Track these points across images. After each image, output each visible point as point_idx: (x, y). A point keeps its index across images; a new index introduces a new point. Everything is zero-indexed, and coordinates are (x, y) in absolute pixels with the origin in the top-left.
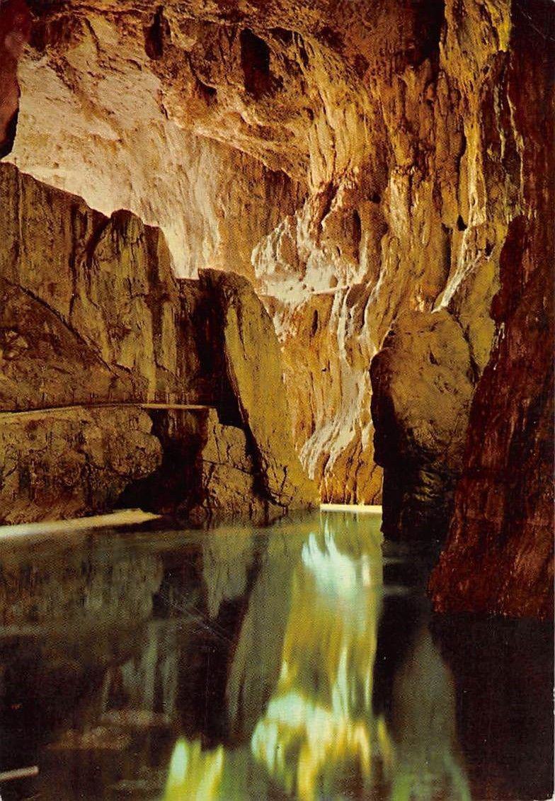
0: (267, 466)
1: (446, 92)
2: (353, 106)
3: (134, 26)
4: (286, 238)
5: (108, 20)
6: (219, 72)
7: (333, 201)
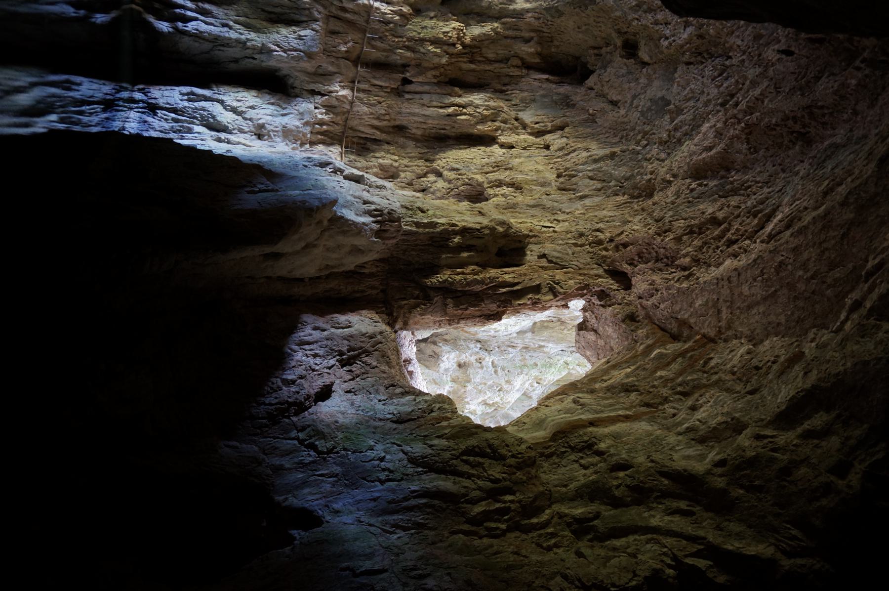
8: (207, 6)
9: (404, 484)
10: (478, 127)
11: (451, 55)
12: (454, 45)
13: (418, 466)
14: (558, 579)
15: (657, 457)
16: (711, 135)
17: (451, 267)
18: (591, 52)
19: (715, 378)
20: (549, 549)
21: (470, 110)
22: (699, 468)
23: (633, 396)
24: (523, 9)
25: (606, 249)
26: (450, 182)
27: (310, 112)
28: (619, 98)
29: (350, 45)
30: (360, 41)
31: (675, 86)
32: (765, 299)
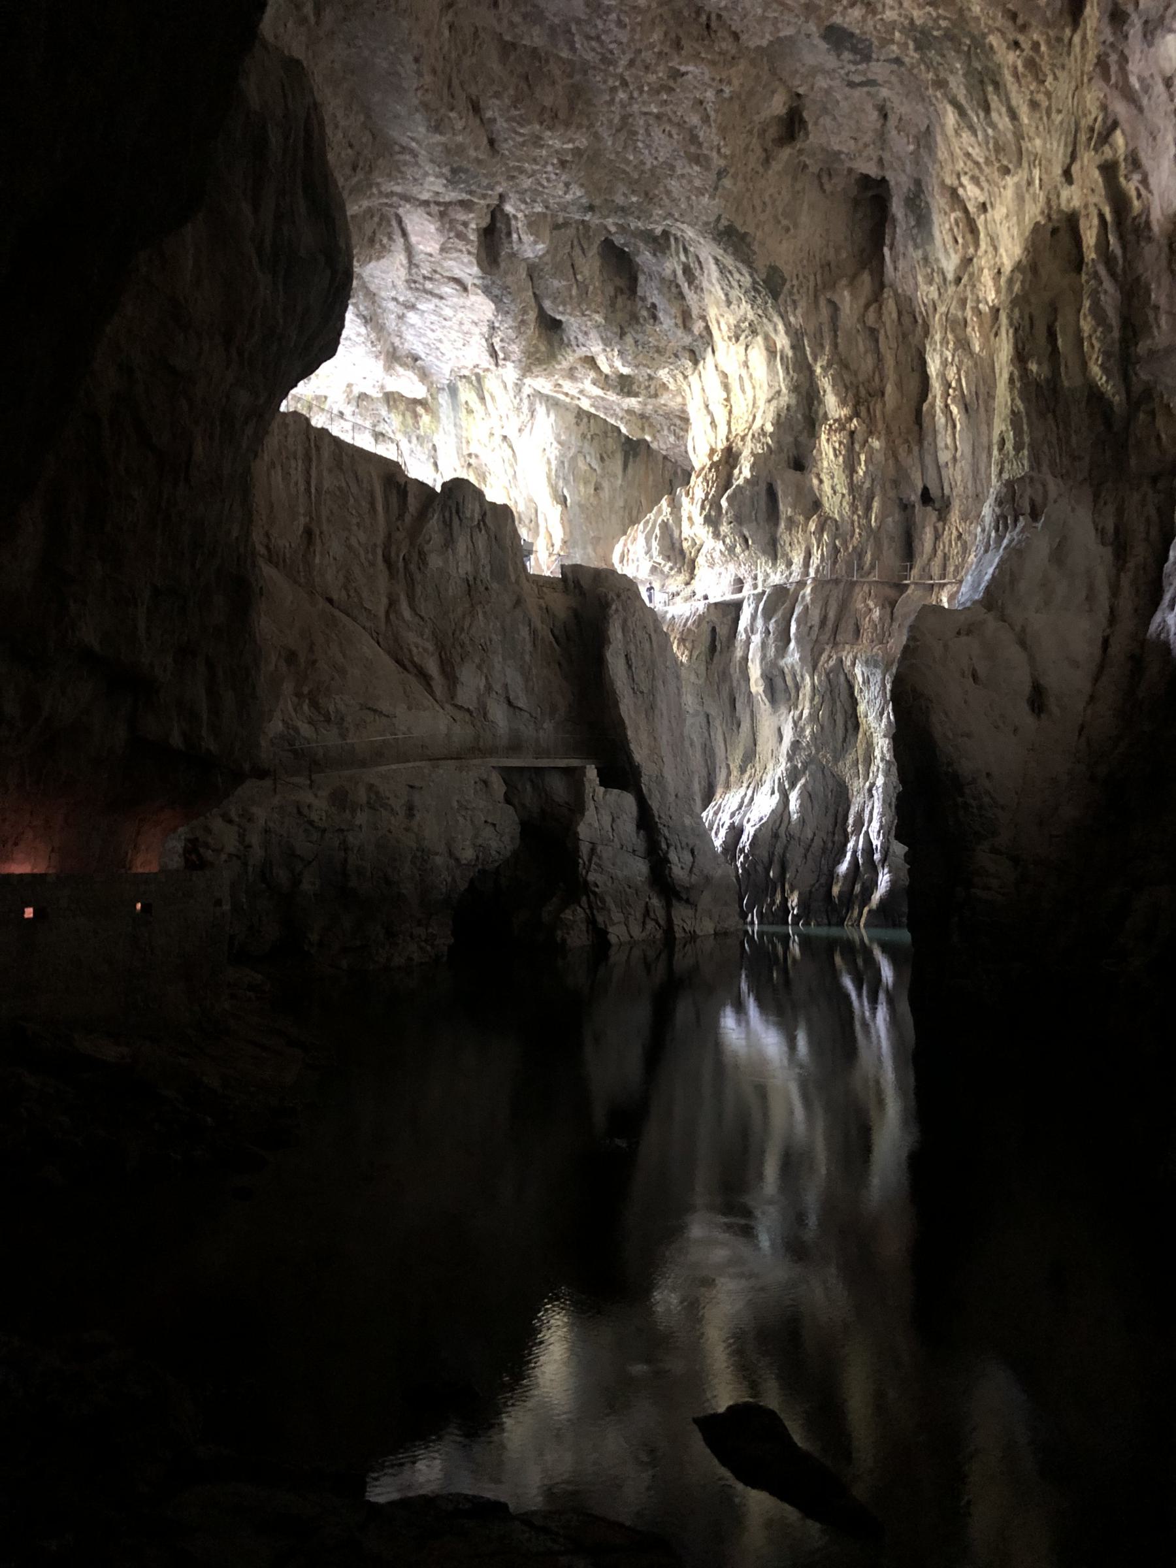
0: (668, 846)
1: (895, 315)
2: (760, 339)
3: (465, 224)
4: (665, 525)
5: (429, 214)
6: (571, 297)
7: (736, 472)
8: (851, 821)
10: (977, 349)
12: (852, 433)
17: (1084, 365)
18: (828, 187)
21: (951, 374)
24: (787, 333)
25: (1036, 46)
28: (869, 107)
29: (871, 604)
30: (866, 588)
31: (782, 34)
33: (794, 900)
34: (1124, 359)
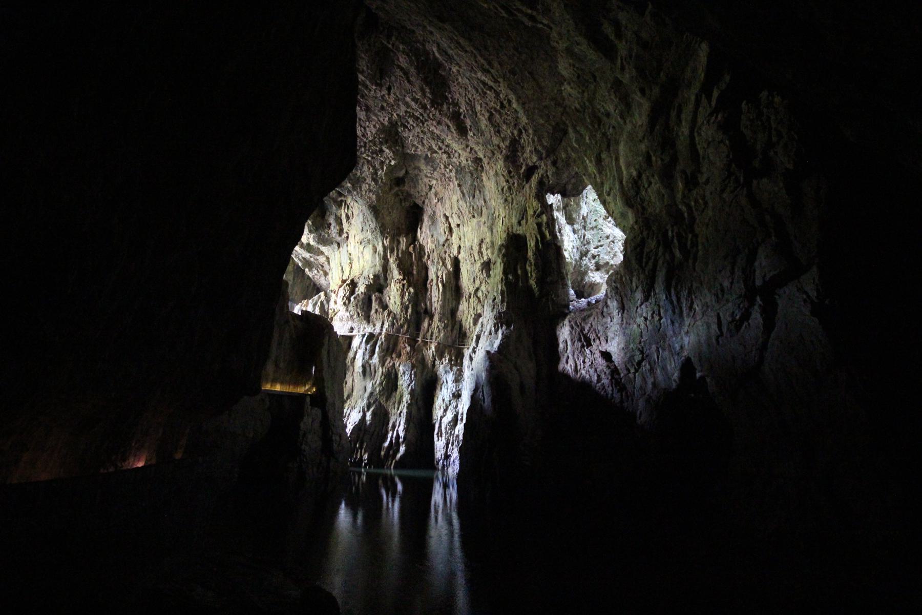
2: (371, 246)
4: (322, 303)
8: (390, 425)
9: (662, 303)
11: (409, 286)
12: (403, 285)
13: (650, 295)
14: (725, 195)
15: (641, 134)
16: (441, 127)
19: (587, 104)
20: (706, 203)
21: (440, 274)
22: (647, 106)
23: (604, 156)
25: (514, 184)
26: (481, 283)
27: (445, 367)
32: (534, 79)
33: (366, 457)
34: (541, 281)
